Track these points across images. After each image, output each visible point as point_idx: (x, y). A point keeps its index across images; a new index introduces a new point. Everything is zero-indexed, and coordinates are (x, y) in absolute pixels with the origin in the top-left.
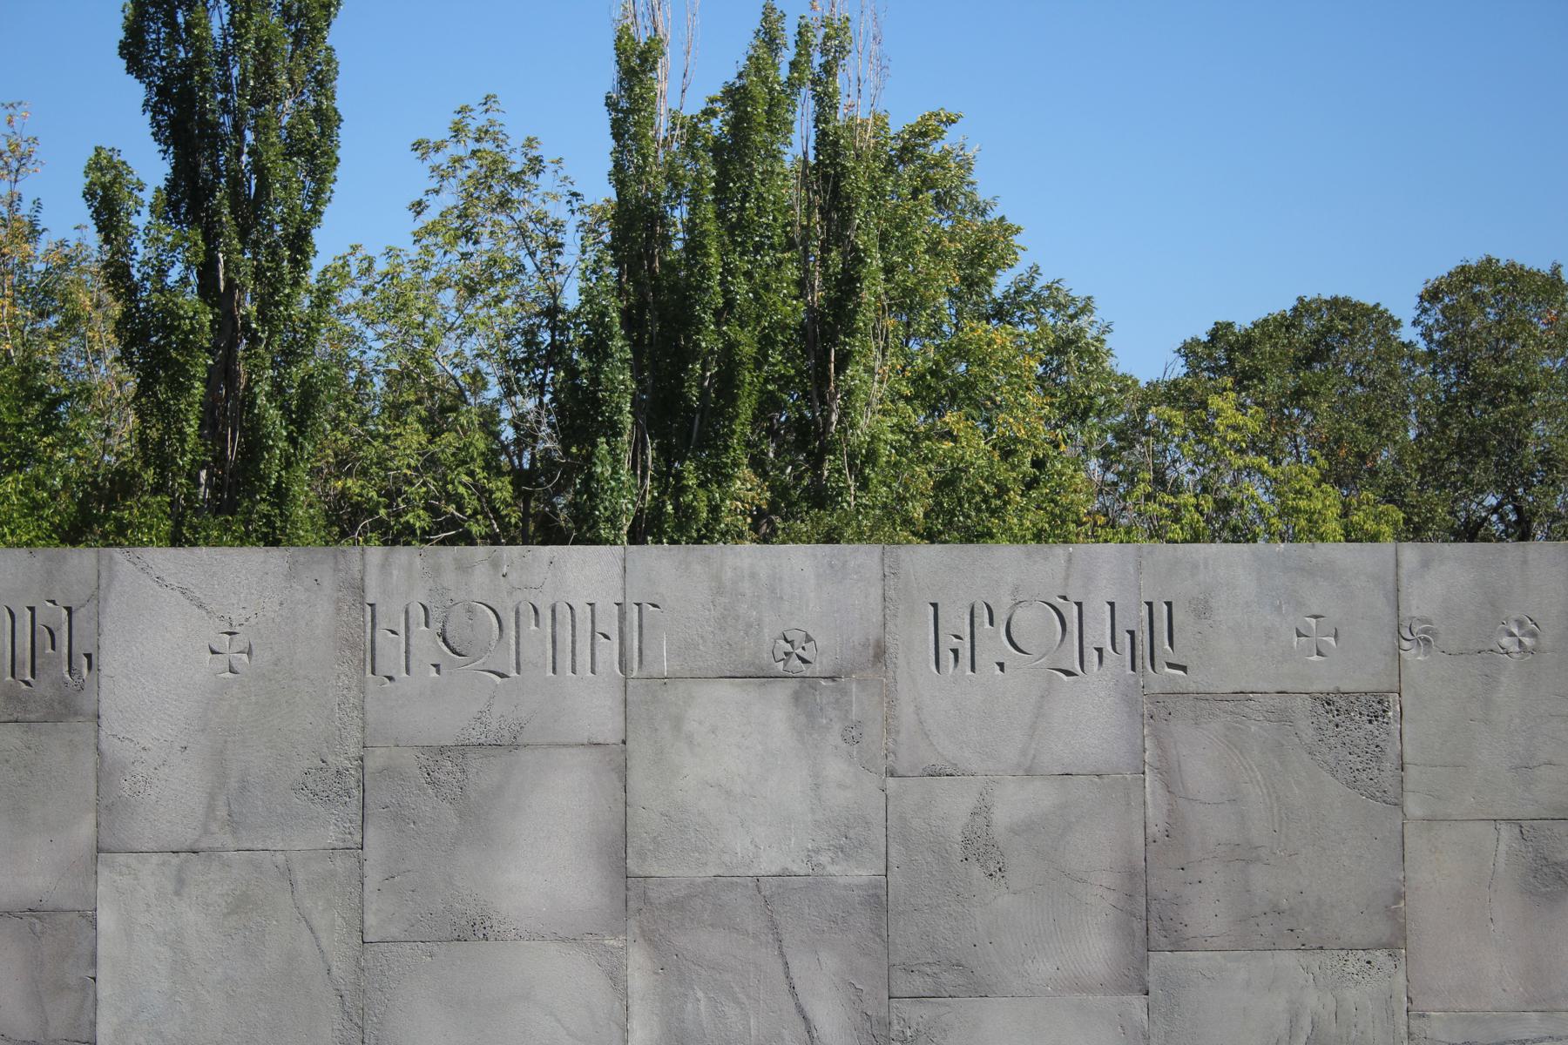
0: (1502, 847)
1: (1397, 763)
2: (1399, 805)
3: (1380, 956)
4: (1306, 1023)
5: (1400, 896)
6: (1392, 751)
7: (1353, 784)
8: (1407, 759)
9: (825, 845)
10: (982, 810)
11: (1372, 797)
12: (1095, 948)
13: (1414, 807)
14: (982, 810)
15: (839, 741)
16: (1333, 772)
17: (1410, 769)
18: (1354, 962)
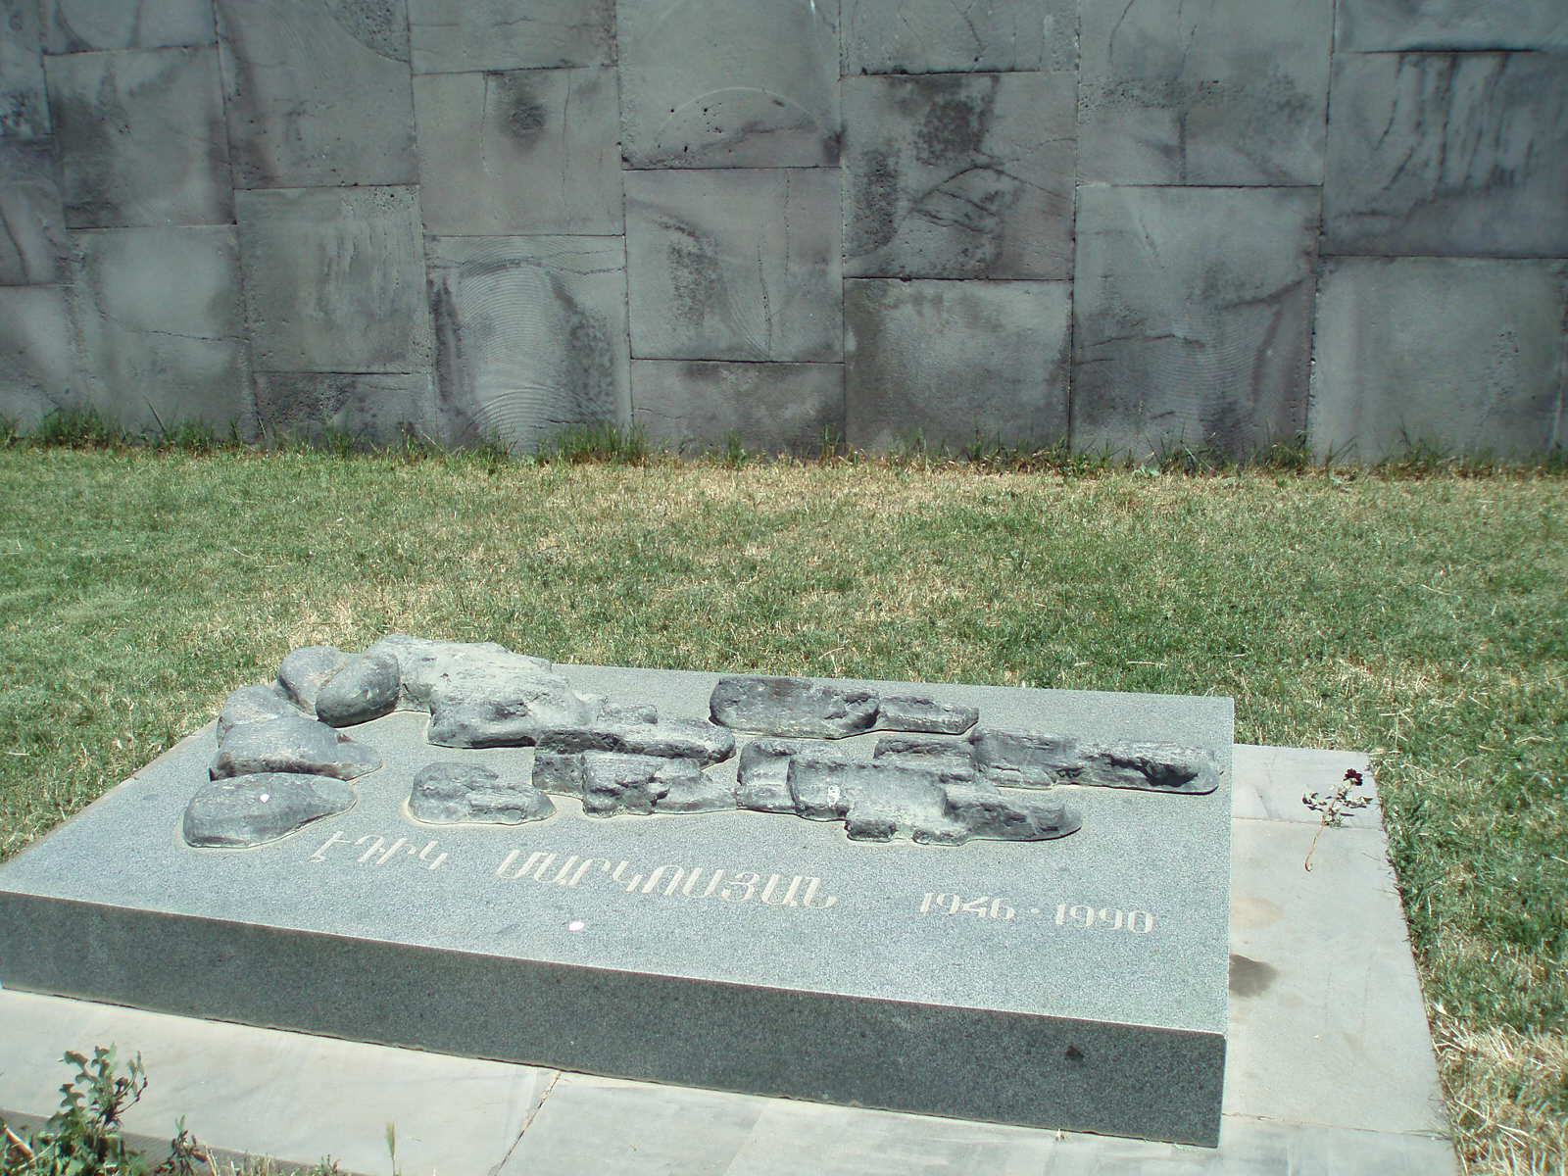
0: (490, 95)
1: (403, 24)
2: (409, 62)
3: (400, 191)
4: (349, 246)
5: (412, 139)
6: (399, 18)
7: (370, 45)
8: (412, 19)
9: (10, 112)
10: (108, 80)
11: (387, 55)
12: (198, 189)
13: (420, 64)
14: (108, 80)
15: (8, 29)
16: (355, 35)
17: (415, 29)
18: (382, 195)
